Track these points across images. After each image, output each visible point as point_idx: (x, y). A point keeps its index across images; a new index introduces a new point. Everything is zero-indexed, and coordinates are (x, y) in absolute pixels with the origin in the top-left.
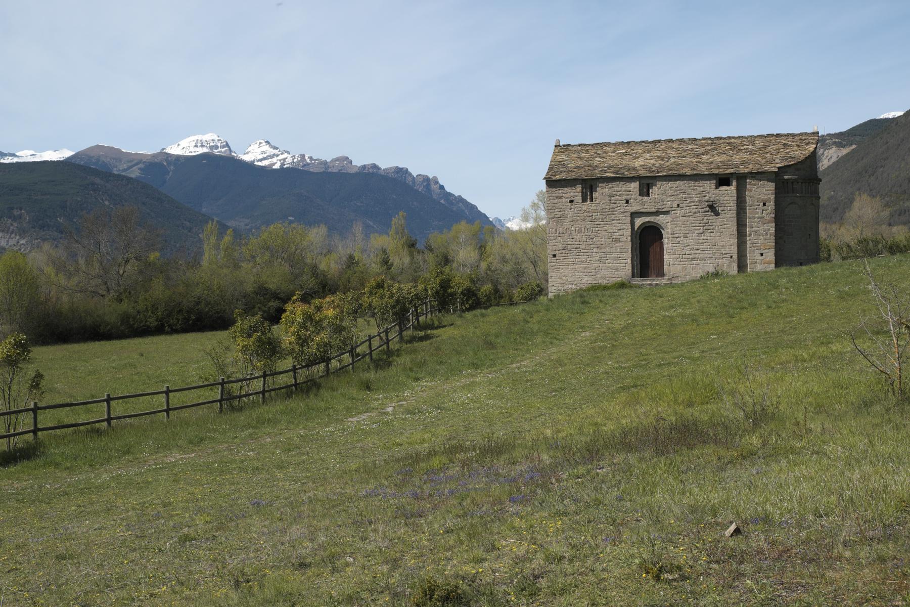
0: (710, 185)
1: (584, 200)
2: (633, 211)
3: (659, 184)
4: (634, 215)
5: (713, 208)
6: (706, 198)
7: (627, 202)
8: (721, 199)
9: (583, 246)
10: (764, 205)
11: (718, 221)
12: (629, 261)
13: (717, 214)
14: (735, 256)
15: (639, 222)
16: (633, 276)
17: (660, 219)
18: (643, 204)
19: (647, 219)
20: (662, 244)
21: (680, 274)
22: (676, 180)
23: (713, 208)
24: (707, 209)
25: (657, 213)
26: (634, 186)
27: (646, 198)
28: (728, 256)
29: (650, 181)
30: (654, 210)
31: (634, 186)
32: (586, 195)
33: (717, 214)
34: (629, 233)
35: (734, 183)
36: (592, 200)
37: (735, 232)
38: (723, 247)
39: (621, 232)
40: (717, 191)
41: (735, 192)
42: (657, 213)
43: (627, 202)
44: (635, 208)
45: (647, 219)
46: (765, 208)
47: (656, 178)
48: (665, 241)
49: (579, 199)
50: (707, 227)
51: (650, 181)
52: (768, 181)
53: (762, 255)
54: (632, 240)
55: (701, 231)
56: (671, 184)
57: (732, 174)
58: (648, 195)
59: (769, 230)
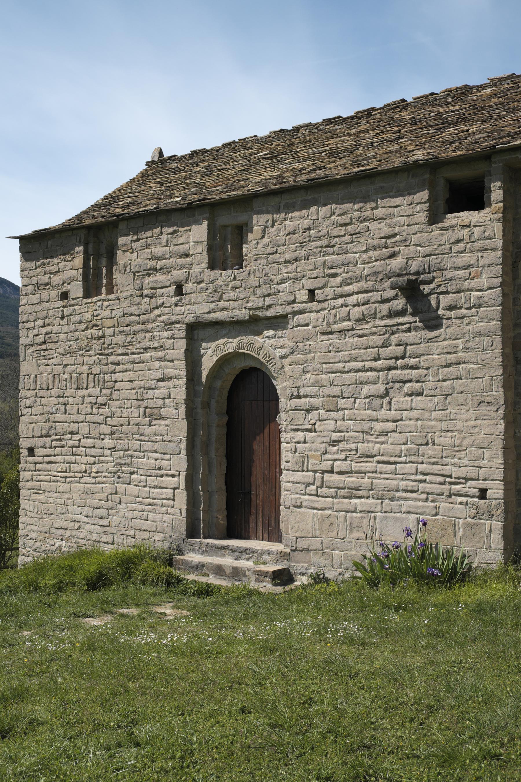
0: (407, 210)
1: (91, 289)
2: (190, 318)
3: (259, 221)
4: (197, 331)
5: (415, 295)
6: (397, 263)
7: (179, 290)
8: (448, 262)
9: (84, 428)
11: (434, 350)
12: (182, 481)
13: (432, 322)
14: (496, 491)
15: (210, 354)
16: (192, 532)
17: (267, 345)
18: (218, 295)
19: (230, 345)
20: (278, 432)
21: (315, 543)
22: (305, 206)
23: (415, 295)
24: (400, 303)
25: (254, 324)
26: (198, 234)
27: (224, 276)
28: (472, 488)
29: (241, 218)
30: (243, 314)
31: (198, 234)
32: (98, 276)
33: (432, 322)
34: (181, 394)
35: (496, 193)
36: (110, 291)
37: (498, 394)
39: (162, 390)
40: (435, 233)
41: (498, 229)
42: (254, 324)
43: (179, 290)
44: (196, 308)
45: (230, 345)
47: (249, 202)
48: (283, 419)
49: (76, 289)
50: (397, 372)
51: (241, 218)
54: (190, 415)
55: (380, 388)
56: (297, 219)
57: (488, 156)
58: (239, 262)
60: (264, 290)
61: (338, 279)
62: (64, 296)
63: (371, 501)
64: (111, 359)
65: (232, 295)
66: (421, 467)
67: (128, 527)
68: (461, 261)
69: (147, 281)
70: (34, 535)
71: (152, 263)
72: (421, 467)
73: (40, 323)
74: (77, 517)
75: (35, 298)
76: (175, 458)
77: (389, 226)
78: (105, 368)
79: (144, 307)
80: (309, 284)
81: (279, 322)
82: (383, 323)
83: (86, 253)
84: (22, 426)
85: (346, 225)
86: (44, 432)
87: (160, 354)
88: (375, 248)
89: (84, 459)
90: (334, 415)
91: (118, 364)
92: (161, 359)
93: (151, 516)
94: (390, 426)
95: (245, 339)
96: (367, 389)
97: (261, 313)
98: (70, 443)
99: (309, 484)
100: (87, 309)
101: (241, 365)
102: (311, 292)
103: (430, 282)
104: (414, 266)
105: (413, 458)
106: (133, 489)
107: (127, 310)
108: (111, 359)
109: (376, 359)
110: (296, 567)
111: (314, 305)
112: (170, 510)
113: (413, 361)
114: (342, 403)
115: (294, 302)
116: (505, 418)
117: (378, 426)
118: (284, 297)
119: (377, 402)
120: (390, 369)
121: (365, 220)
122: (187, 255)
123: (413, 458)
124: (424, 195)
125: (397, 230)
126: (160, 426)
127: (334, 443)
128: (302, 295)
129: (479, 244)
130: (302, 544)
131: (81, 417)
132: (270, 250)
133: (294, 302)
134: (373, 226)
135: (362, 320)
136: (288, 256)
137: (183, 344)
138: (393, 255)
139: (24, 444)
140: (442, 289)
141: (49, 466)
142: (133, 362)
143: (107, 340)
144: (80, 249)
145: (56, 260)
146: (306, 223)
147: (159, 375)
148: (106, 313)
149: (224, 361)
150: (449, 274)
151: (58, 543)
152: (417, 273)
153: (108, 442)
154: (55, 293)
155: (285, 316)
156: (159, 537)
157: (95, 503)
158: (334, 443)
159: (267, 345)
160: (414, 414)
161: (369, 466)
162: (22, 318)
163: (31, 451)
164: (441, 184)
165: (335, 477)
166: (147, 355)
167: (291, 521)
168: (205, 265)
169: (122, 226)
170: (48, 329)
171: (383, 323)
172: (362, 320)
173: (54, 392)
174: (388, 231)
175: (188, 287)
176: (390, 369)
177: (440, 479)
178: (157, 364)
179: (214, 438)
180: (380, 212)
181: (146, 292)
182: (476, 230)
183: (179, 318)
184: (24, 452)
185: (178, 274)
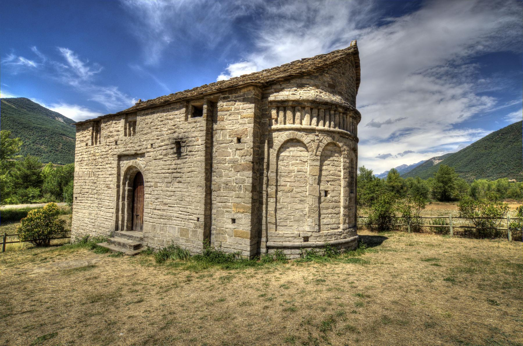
0: (178, 116)
2: (119, 153)
3: (139, 118)
4: (121, 157)
6: (175, 135)
10: (239, 140)
17: (140, 163)
26: (121, 124)
28: (194, 217)
30: (133, 152)
35: (205, 111)
38: (190, 203)
42: (135, 156)
44: (121, 150)
46: (239, 146)
49: (90, 143)
52: (245, 100)
53: (234, 221)
59: (244, 181)
60: (139, 144)
61: (159, 140)
62: (87, 145)
63: (166, 220)
64: (98, 167)
65: (130, 145)
66: (181, 209)
67: (100, 226)
68: (193, 135)
69: (108, 140)
70: (75, 228)
71: (110, 134)
72: (181, 209)
73: (80, 154)
74: (87, 222)
75: (79, 145)
76: (113, 202)
77: (174, 122)
78: (96, 170)
79: (107, 149)
80: (151, 142)
81: (142, 155)
82: (171, 156)
83: (93, 130)
84: (74, 190)
85: (162, 121)
86: (79, 192)
87: (110, 165)
88: (170, 129)
89: (89, 202)
90: (157, 189)
91: (99, 169)
92: (110, 167)
93: (106, 223)
94: (172, 193)
95: (134, 161)
96: (166, 180)
97: (139, 152)
98: (86, 196)
99: (149, 213)
100: (92, 150)
101: (135, 170)
102: (152, 145)
103: (185, 142)
104: (180, 136)
105: (179, 206)
106: (102, 213)
107: (102, 150)
108: (98, 167)
109: (169, 169)
110: (144, 243)
111: (152, 150)
112: (111, 221)
113: (179, 170)
114: (159, 185)
115: (147, 148)
116: (206, 192)
117: (169, 193)
118: (144, 146)
119: (169, 185)
120: (173, 173)
121: (167, 119)
122: (118, 131)
123: (179, 206)
124: (184, 110)
125: (176, 123)
126: (109, 191)
127: (157, 199)
128: (149, 146)
129: (199, 128)
130: (147, 235)
131: (89, 187)
132: (141, 130)
133: (147, 148)
134: (169, 121)
135: (166, 155)
136: (145, 132)
137: (116, 162)
138: (175, 132)
139: (75, 196)
140: (188, 145)
141: (80, 204)
142: (103, 168)
143: (97, 160)
144: (91, 128)
145: (85, 132)
146: (151, 120)
147: (110, 173)
148: (97, 151)
149: (130, 168)
150: (190, 139)
151: (82, 231)
152: (181, 139)
153: (96, 196)
154: (85, 144)
155: (144, 153)
156: (108, 230)
157: (92, 217)
158: (157, 199)
159: (140, 163)
160: (179, 189)
161: (166, 207)
162: (76, 152)
163: (76, 198)
164: (190, 107)
165: (156, 211)
166: (107, 166)
167: (147, 226)
168: (123, 135)
169: (102, 121)
170: (82, 156)
171: (171, 156)
172: (166, 155)
173: (83, 178)
174: (173, 123)
175: (119, 142)
176: (173, 173)
177: (186, 213)
178: (110, 169)
179: (126, 195)
180: (171, 117)
181: (108, 144)
182: (198, 123)
183: (115, 153)
184: (74, 199)
185: (116, 138)
